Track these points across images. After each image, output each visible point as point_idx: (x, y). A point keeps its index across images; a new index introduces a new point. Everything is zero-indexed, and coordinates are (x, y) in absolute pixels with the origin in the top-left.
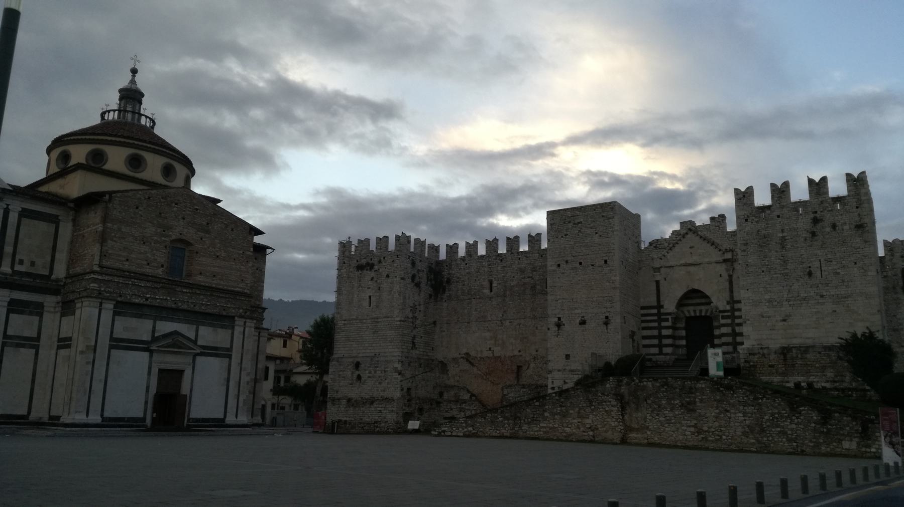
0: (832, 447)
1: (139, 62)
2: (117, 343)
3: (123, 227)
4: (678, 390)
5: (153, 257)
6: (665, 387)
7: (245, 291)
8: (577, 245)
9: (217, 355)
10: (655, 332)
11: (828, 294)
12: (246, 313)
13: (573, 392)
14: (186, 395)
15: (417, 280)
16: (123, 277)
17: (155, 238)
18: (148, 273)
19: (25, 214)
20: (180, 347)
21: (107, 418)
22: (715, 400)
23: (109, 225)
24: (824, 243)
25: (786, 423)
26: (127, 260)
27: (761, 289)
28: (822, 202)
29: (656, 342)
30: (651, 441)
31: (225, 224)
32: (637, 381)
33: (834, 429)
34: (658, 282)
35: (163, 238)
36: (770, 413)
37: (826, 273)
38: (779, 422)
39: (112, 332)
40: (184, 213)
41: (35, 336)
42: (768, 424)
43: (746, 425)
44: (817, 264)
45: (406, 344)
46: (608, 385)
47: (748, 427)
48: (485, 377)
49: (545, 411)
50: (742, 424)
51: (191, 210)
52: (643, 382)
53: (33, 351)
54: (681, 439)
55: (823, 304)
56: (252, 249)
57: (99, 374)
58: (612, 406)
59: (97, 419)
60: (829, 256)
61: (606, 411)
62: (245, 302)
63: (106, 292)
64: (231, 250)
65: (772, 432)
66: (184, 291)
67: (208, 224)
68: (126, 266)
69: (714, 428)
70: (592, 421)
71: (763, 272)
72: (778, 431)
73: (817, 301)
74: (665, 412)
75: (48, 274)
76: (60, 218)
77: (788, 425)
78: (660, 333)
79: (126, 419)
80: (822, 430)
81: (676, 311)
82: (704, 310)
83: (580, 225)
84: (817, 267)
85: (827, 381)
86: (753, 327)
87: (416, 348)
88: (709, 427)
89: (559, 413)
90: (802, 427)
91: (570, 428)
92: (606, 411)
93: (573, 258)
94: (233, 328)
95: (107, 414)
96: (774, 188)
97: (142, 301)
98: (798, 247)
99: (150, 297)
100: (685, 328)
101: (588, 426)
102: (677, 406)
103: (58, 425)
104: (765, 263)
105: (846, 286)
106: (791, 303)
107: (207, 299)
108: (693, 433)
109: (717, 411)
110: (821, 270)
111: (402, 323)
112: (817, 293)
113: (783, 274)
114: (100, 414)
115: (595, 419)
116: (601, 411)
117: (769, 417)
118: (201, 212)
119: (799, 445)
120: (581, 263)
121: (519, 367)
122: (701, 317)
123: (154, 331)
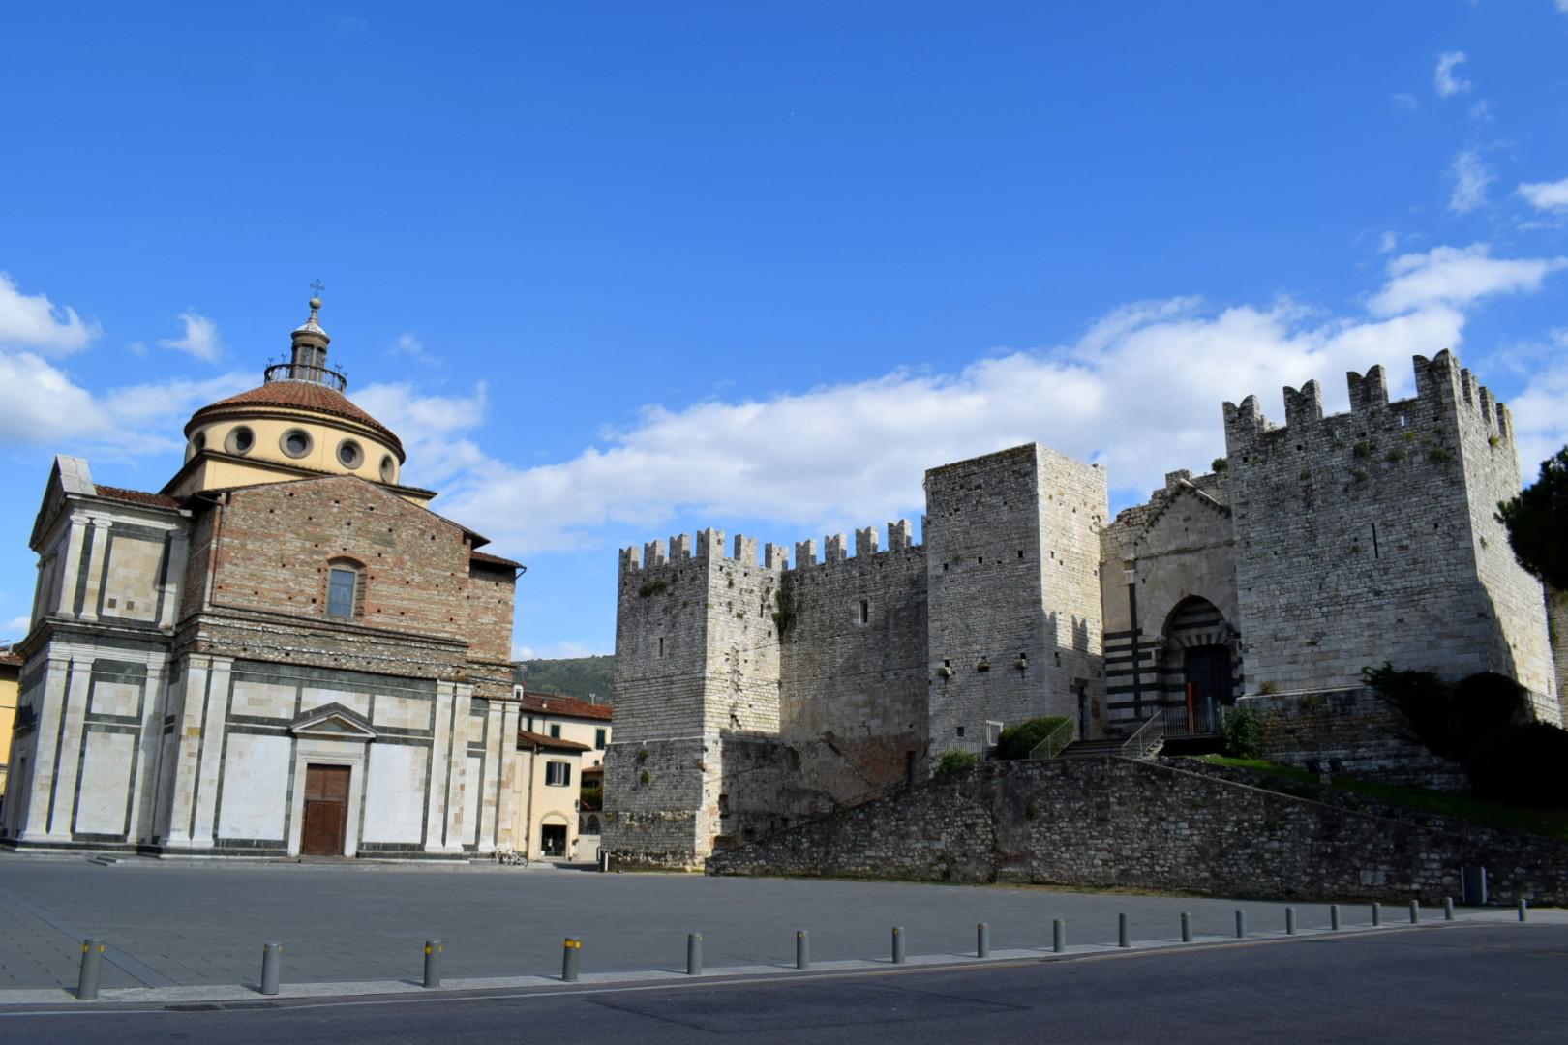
0: (1343, 883)
2: (238, 724)
3: (249, 542)
4: (1081, 783)
5: (298, 588)
6: (1062, 778)
8: (973, 527)
9: (406, 742)
10: (1129, 680)
11: (1390, 588)
13: (916, 794)
16: (247, 620)
17: (302, 557)
18: (291, 612)
19: (116, 530)
22: (1144, 799)
23: (226, 540)
25: (1262, 839)
26: (256, 593)
29: (1129, 697)
31: (420, 529)
32: (1016, 769)
34: (1132, 587)
35: (315, 557)
37: (1386, 549)
38: (1250, 838)
39: (229, 707)
40: (349, 515)
42: (1231, 841)
43: (1194, 845)
45: (716, 720)
46: (970, 779)
47: (1197, 847)
48: (856, 774)
49: (872, 829)
50: (1188, 844)
52: (1025, 770)
54: (1086, 874)
55: (1380, 608)
58: (977, 816)
59: (209, 843)
60: (1389, 516)
61: (967, 826)
62: (456, 654)
64: (432, 571)
65: (1236, 857)
66: (351, 639)
67: (390, 530)
68: (255, 603)
72: (1247, 854)
74: (1060, 825)
75: (152, 620)
77: (1264, 842)
78: (1137, 680)
80: (1323, 849)
81: (1165, 637)
82: (1213, 635)
84: (1369, 539)
88: (1133, 850)
89: (894, 831)
90: (1289, 844)
91: (911, 857)
92: (967, 826)
95: (223, 834)
96: (1289, 396)
98: (1333, 504)
99: (293, 650)
100: (1184, 670)
101: (939, 854)
102: (1080, 813)
105: (1421, 571)
109: (1147, 819)
110: (1376, 544)
114: (211, 832)
117: (1233, 827)
118: (379, 512)
119: (1284, 879)
121: (910, 755)
122: (1209, 646)
123: (298, 704)
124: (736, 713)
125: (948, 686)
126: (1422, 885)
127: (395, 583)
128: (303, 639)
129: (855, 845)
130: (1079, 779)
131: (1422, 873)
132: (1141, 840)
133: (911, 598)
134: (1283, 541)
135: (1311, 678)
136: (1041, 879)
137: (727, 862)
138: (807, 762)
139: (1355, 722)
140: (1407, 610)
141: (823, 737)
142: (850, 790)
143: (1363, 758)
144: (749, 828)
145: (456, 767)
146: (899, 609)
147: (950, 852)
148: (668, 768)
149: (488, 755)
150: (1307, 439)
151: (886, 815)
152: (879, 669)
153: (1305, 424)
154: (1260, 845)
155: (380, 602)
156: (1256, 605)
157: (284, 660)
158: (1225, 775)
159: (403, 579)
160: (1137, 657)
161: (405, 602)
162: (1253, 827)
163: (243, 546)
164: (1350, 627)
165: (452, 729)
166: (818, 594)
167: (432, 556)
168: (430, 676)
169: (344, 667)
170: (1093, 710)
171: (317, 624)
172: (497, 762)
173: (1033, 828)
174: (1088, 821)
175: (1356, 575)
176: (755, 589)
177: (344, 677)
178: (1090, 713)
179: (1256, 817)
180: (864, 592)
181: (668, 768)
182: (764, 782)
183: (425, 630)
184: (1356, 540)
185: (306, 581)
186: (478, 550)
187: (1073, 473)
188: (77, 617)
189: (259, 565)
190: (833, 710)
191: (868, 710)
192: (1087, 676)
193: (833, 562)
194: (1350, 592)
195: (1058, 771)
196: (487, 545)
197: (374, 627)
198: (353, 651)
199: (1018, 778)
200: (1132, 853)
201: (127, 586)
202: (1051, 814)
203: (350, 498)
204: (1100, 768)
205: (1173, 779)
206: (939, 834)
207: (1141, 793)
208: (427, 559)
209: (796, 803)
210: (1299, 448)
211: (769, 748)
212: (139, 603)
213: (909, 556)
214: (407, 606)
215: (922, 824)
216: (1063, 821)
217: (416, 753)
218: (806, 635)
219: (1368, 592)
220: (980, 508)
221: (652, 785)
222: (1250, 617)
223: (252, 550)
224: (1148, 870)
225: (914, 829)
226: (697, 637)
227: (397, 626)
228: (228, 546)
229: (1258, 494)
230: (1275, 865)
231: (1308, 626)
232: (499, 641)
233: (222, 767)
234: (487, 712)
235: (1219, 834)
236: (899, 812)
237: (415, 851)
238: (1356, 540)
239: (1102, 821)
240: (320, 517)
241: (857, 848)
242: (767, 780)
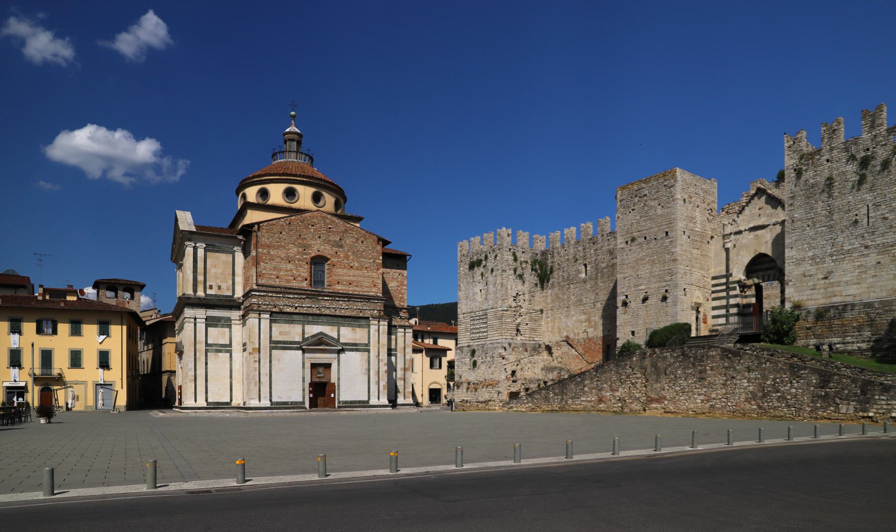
3: (271, 250)
4: (692, 359)
5: (298, 273)
6: (681, 357)
7: (378, 294)
8: (642, 219)
9: (357, 350)
11: (874, 243)
12: (380, 313)
13: (607, 367)
14: (334, 383)
15: (519, 272)
17: (298, 257)
18: (295, 286)
21: (275, 402)
23: (260, 250)
24: (873, 186)
25: (786, 388)
26: (278, 277)
27: (805, 246)
28: (875, 136)
30: (668, 410)
31: (355, 238)
32: (658, 352)
33: (833, 392)
35: (304, 256)
36: (772, 378)
37: (874, 220)
38: (779, 387)
40: (319, 232)
41: (228, 343)
43: (749, 391)
44: (864, 211)
46: (634, 359)
47: (751, 392)
49: (585, 386)
50: (746, 391)
51: (325, 229)
52: (663, 353)
53: (228, 354)
55: (867, 255)
56: (381, 258)
58: (637, 378)
61: (633, 384)
63: (264, 305)
64: (363, 260)
65: (772, 398)
68: (277, 282)
69: (720, 395)
70: (621, 393)
71: (808, 226)
72: (778, 396)
73: (860, 254)
74: (680, 382)
75: (231, 294)
79: (290, 403)
80: (820, 393)
83: (645, 197)
85: (864, 342)
86: (794, 288)
89: (596, 387)
92: (633, 384)
93: (638, 233)
94: (369, 326)
98: (845, 194)
99: (298, 306)
103: (229, 408)
104: (811, 216)
107: (345, 304)
108: (702, 401)
109: (725, 378)
110: (868, 217)
111: (504, 312)
112: (862, 244)
113: (828, 226)
115: (623, 391)
116: (628, 384)
117: (771, 382)
118: (334, 230)
120: (645, 238)
123: (303, 334)
124: (519, 328)
125: (627, 309)
126: (875, 413)
127: (345, 267)
129: (576, 394)
130: (691, 357)
131: (875, 406)
132: (722, 389)
133: (610, 261)
134: (813, 218)
135: (823, 298)
136: (670, 410)
137: (513, 405)
138: (556, 352)
139: (846, 323)
140: (884, 256)
141: (564, 339)
142: (577, 366)
143: (849, 343)
144: (527, 387)
145: (382, 361)
146: (603, 268)
147: (624, 397)
148: (486, 358)
149: (398, 355)
150: (833, 155)
151: (592, 379)
152: (592, 301)
153: (833, 145)
154: (785, 391)
155: (339, 278)
156: (795, 257)
157: (295, 311)
158: (770, 353)
159: (349, 266)
160: (728, 289)
161: (351, 277)
162: (782, 382)
163: (269, 253)
164: (848, 268)
165: (379, 343)
166: (562, 262)
167: (363, 252)
168: (366, 316)
169: (324, 313)
170: (703, 319)
171: (309, 292)
172: (403, 358)
173: (666, 384)
174: (695, 379)
175: (854, 237)
176: (529, 260)
177: (325, 319)
178: (702, 321)
179: (784, 376)
180: (585, 259)
181: (486, 358)
182: (535, 363)
183: (362, 291)
184: (856, 215)
185: (301, 269)
186: (386, 247)
187: (698, 184)
188: (195, 295)
189: (278, 263)
190: (569, 324)
191: (587, 324)
192: (701, 301)
193: (569, 243)
194: (850, 247)
195: (679, 354)
196: (390, 244)
197: (337, 292)
198: (327, 305)
199: (659, 357)
200: (717, 396)
201: (216, 278)
202: (675, 376)
203: (319, 223)
204: (702, 351)
205: (740, 356)
206: (618, 388)
207: (723, 364)
208: (360, 254)
209: (551, 373)
210: (828, 161)
211: (537, 346)
212: (223, 286)
213: (609, 238)
214: (353, 280)
215: (609, 383)
216: (681, 380)
217: (362, 356)
218: (555, 284)
219: (861, 246)
220: (646, 208)
221: (479, 367)
222: (791, 264)
223: (274, 255)
224: (725, 404)
225: (605, 386)
226: (498, 288)
227: (349, 291)
228: (262, 253)
229: (802, 190)
230: (793, 402)
231: (824, 268)
232: (400, 295)
234: (396, 333)
235: (763, 385)
236: (598, 377)
237: (365, 404)
238: (856, 215)
239: (702, 379)
241: (577, 396)
242: (536, 362)
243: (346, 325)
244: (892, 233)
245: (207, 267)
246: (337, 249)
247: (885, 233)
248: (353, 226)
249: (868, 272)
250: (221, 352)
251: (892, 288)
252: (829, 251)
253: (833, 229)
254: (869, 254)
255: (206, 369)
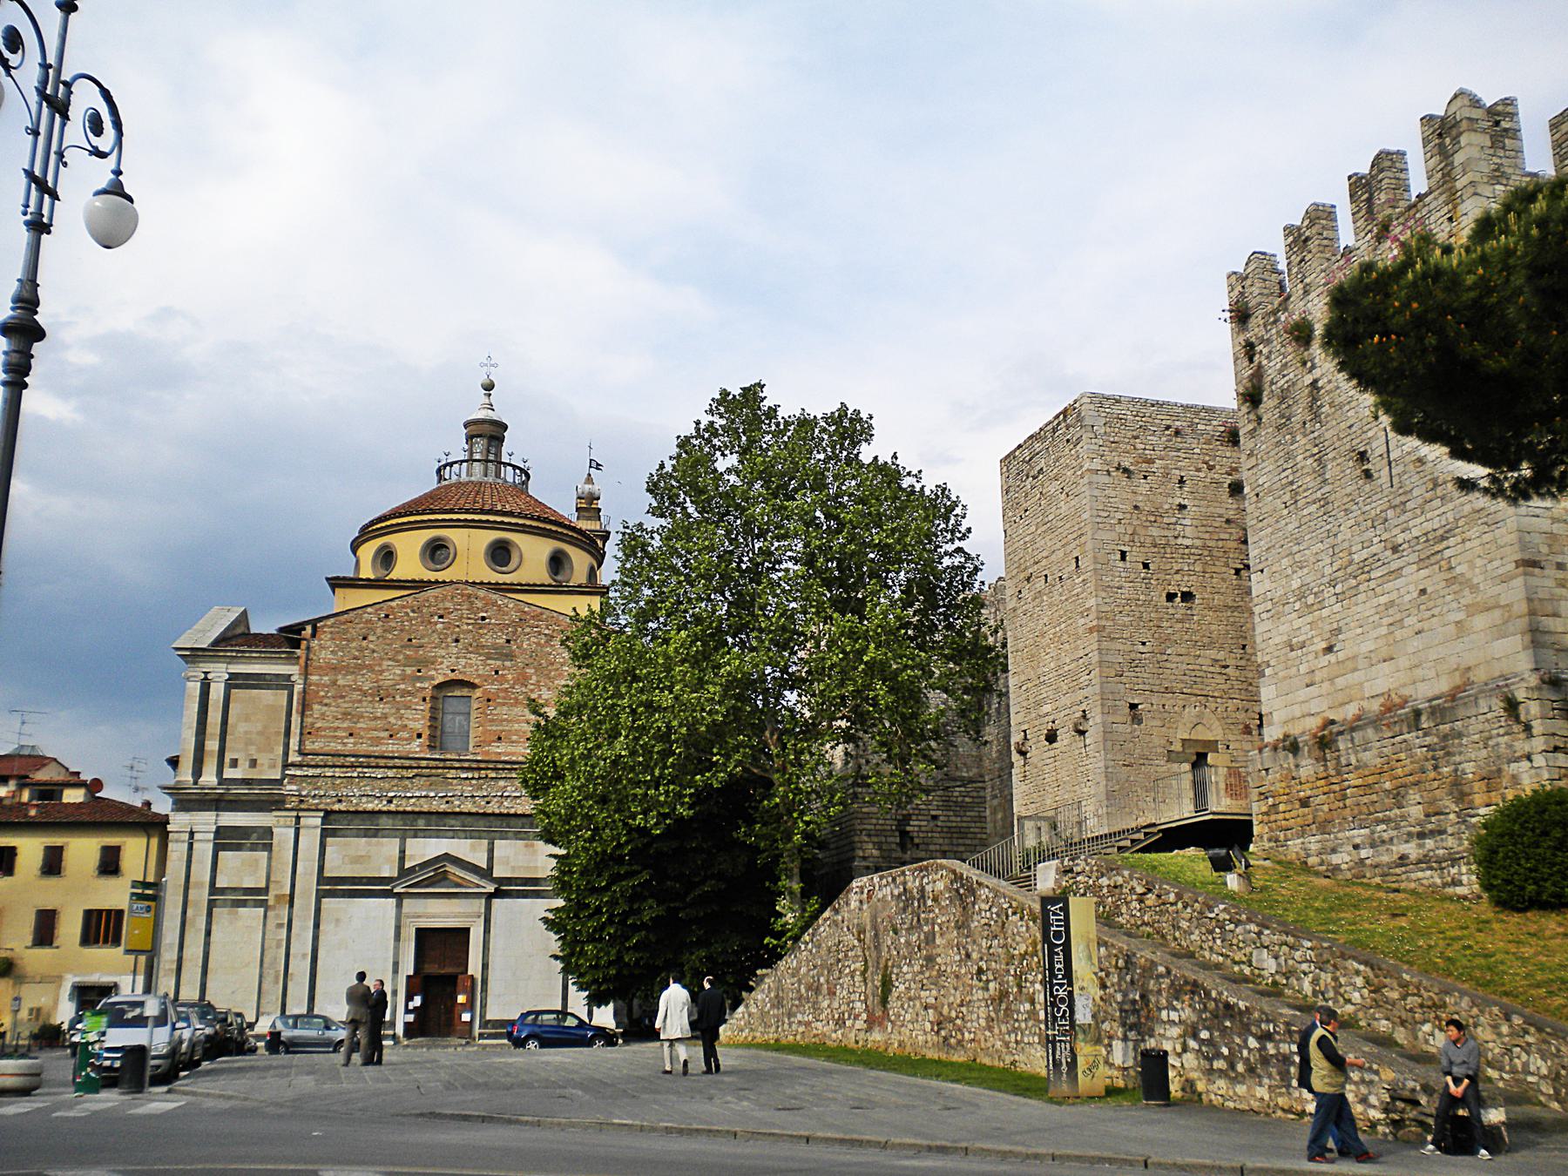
1: (495, 366)
2: (332, 887)
17: (403, 686)
19: (235, 682)
20: (458, 885)
26: (351, 735)
39: (321, 868)
57: (302, 945)
66: (464, 776)
67: (508, 641)
68: (350, 745)
76: (293, 679)
87: (918, 845)
97: (381, 806)
106: (1339, 589)
123: (402, 859)
128: (407, 782)
157: (385, 809)
163: (334, 683)
169: (458, 810)
171: (424, 763)
175: (1369, 523)
177: (455, 823)
185: (408, 714)
188: (196, 783)
189: (353, 702)
194: (1365, 554)
201: (249, 742)
212: (263, 760)
228: (317, 685)
233: (316, 938)
240: (422, 637)
243: (510, 835)
244: (1437, 502)
245: (230, 722)
246: (499, 663)
247: (1427, 502)
248: (539, 610)
249: (1408, 621)
250: (245, 906)
251: (1459, 665)
252: (1328, 570)
253: (1330, 507)
254: (1402, 568)
255: (207, 944)
